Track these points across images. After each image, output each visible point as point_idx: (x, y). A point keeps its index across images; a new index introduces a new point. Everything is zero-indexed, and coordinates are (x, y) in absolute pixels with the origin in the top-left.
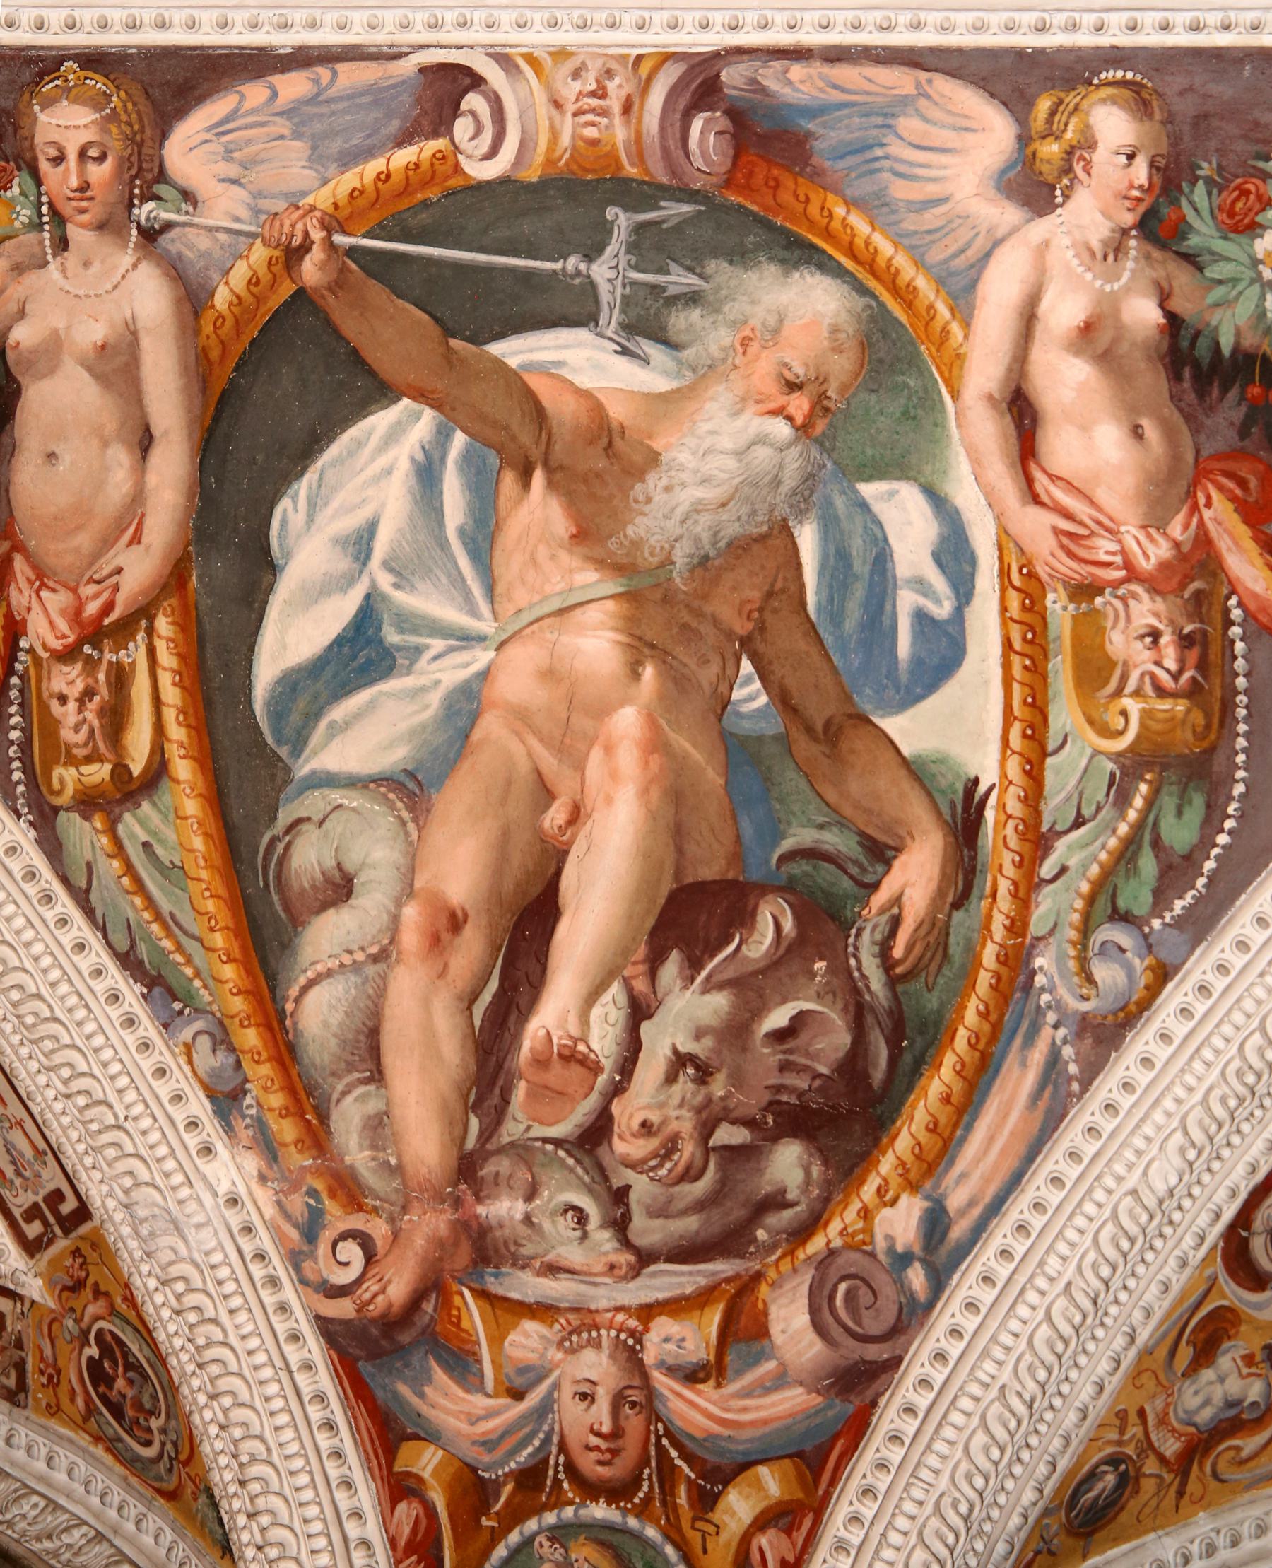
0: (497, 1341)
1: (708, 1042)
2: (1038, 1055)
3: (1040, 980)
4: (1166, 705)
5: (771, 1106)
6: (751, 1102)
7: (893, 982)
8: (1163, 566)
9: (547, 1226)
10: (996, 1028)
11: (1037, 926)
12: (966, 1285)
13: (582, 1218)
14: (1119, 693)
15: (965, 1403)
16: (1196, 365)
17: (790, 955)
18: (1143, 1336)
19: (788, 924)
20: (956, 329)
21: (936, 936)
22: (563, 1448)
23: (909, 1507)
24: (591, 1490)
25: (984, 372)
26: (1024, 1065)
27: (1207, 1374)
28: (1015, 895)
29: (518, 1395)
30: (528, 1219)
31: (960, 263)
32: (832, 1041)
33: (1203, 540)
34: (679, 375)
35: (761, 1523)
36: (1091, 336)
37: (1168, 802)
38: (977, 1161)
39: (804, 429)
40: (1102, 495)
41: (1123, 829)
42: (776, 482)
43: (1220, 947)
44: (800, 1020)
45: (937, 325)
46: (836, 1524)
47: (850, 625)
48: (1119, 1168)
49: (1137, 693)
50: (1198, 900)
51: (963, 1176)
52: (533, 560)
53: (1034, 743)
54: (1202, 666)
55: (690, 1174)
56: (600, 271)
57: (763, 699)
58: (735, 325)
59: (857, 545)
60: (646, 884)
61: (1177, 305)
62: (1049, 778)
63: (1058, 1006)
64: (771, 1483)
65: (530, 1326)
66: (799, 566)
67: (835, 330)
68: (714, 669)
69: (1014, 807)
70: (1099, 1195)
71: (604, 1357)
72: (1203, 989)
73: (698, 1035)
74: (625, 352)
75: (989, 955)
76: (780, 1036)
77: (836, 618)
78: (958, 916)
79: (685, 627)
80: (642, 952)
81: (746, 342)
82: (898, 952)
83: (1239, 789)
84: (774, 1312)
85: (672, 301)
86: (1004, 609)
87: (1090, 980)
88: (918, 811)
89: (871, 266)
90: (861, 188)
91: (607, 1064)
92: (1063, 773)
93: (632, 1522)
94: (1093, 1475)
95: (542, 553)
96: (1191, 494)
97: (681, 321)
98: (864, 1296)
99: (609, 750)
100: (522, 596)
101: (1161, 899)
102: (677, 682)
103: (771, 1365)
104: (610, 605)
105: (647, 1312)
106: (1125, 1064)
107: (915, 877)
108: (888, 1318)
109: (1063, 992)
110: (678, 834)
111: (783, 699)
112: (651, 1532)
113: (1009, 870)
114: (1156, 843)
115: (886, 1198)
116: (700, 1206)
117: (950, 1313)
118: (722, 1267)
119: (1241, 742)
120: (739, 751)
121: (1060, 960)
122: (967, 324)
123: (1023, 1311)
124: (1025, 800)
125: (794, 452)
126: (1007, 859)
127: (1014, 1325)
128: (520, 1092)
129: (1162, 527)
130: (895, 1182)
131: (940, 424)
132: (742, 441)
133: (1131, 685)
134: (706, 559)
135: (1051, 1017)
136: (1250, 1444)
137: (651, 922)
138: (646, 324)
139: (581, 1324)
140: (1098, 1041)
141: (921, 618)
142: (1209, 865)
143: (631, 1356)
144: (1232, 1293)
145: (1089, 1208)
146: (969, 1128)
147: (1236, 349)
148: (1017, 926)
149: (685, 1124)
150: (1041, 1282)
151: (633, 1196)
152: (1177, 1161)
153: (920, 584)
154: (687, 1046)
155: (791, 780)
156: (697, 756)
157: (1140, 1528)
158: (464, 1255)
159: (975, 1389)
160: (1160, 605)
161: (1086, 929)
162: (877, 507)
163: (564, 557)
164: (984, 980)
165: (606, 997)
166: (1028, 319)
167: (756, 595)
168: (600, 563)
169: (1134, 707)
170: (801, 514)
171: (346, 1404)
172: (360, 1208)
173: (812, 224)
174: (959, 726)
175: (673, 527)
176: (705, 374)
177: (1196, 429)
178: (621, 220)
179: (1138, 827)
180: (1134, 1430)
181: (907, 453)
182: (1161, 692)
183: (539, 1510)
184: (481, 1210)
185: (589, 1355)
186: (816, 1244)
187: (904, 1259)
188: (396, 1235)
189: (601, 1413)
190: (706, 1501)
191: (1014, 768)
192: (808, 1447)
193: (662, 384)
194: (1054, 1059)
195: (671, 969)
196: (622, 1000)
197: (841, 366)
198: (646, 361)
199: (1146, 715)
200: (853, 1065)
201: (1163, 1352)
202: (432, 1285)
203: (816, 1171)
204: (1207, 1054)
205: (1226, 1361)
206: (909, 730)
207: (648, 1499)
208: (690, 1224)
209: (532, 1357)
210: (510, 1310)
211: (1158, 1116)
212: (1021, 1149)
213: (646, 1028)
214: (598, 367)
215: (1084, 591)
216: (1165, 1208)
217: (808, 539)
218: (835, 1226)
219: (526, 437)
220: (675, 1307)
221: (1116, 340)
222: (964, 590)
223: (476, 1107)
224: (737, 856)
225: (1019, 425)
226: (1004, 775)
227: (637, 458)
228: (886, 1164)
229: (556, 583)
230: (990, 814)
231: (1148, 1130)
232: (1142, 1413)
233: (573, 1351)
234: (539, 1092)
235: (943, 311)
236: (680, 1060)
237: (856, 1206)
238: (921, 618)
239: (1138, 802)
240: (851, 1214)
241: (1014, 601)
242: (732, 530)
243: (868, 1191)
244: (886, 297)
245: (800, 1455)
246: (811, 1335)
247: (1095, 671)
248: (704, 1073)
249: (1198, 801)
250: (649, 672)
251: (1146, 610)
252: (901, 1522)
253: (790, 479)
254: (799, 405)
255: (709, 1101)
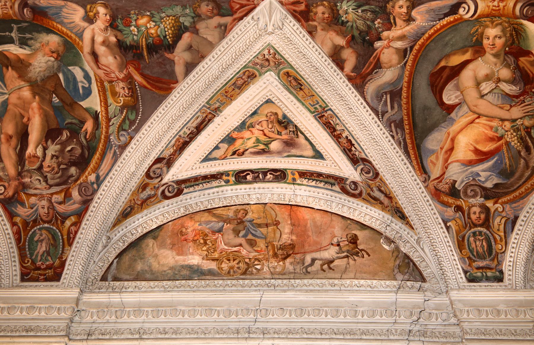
0: (28, 200)
1: (57, 153)
2: (112, 151)
3: (111, 140)
4: (127, 98)
5: (69, 162)
6: (66, 161)
7: (87, 142)
8: (123, 78)
9: (34, 182)
10: (105, 148)
11: (110, 132)
12: (103, 187)
13: (40, 181)
14: (119, 97)
15: (103, 205)
16: (124, 47)
17: (69, 140)
18: (133, 189)
19: (68, 134)
20: (80, 42)
21: (93, 135)
22: (40, 216)
23: (94, 222)
24: (45, 222)
25: (87, 49)
26: (110, 153)
27: (145, 192)
28: (106, 128)
29: (32, 208)
30: (31, 181)
31: (79, 32)
32: (79, 151)
33: (129, 73)
34: (32, 51)
35: (71, 225)
36: (105, 43)
37: (129, 113)
38: (104, 168)
39: (56, 59)
40: (111, 67)
41: (122, 117)
42: (53, 67)
43: (140, 134)
44: (72, 149)
45: (77, 42)
46: (83, 225)
47: (71, 89)
48: (126, 168)
49: (122, 97)
50: (136, 127)
51: (102, 170)
52: (12, 81)
53: (106, 105)
54: (132, 92)
55: (57, 173)
56: (13, 35)
57: (58, 100)
58: (41, 43)
59: (70, 76)
60: (43, 129)
61: (119, 38)
62: (109, 110)
63: (115, 144)
64: (73, 219)
65: (33, 197)
66: (60, 80)
67: (58, 43)
68: (48, 96)
69: (104, 114)
70: (123, 172)
71: (46, 202)
72: (138, 141)
73: (56, 152)
74: (21, 47)
75: (103, 137)
76: (69, 151)
77: (69, 88)
78: (97, 131)
79: (42, 90)
80: (44, 140)
81: (43, 45)
82: (87, 137)
83: (141, 110)
84: (73, 193)
85: (28, 39)
86: (97, 85)
87: (120, 140)
88: (88, 116)
89: (63, 32)
90: (58, 20)
91: (41, 157)
92: (111, 109)
93: (51, 227)
94: (126, 209)
95: (13, 80)
96: (126, 67)
97: (30, 42)
98: (87, 189)
99: (32, 109)
100: (11, 87)
101: (130, 127)
102: (42, 99)
103: (72, 201)
104: (28, 87)
105: (52, 194)
106: (126, 152)
107: (89, 126)
108: (91, 193)
109: (115, 142)
110: (47, 121)
111: (61, 100)
112: (54, 228)
113: (104, 124)
114: (128, 119)
115: (89, 174)
116: (59, 178)
117: (100, 191)
118: (64, 187)
119: (140, 103)
120: (55, 108)
121: (115, 137)
122: (82, 41)
123: (111, 191)
124: (106, 114)
125: (56, 62)
126: (104, 122)
127: (110, 193)
128: (27, 162)
129: (122, 72)
130: (91, 172)
131: (80, 57)
132: (46, 61)
133: (121, 95)
134: (43, 79)
135: (114, 146)
136: (152, 200)
137: (45, 135)
138: (23, 43)
139: (41, 197)
140: (122, 149)
141: (83, 87)
142: (137, 121)
143: (50, 201)
144: (147, 181)
145: (121, 174)
146: (102, 163)
147: (130, 44)
148: (107, 132)
149: (55, 165)
150: (114, 186)
151: (48, 177)
152: (135, 167)
153: (82, 82)
154: (54, 153)
155: (65, 112)
156: (48, 109)
157: (135, 214)
158: (21, 188)
159: (104, 203)
160: (124, 83)
161: (118, 132)
162: (72, 70)
163: (18, 80)
164: (102, 141)
165: (39, 147)
166: (93, 41)
167: (53, 85)
168: (24, 81)
169: (122, 99)
170: (59, 72)
171: (4, 211)
172: (2, 181)
173: (51, 26)
174: (94, 102)
175: (36, 75)
176: (36, 51)
177: (125, 57)
178: (15, 27)
179: (125, 117)
180: (133, 202)
181: (77, 61)
182: (126, 96)
183: (37, 226)
184: (23, 180)
185: (43, 201)
186: (79, 182)
187: (93, 183)
188: (9, 185)
189: (46, 210)
190: (63, 223)
191: (103, 109)
192: (79, 213)
193: (29, 53)
194: (115, 152)
195: (49, 142)
196: (42, 147)
197: (61, 49)
198: (25, 49)
199: (124, 100)
200: (82, 154)
201: (137, 190)
202: (16, 192)
203: (78, 171)
204: (139, 150)
205: (147, 190)
206: (84, 104)
207: (54, 223)
208: (58, 180)
209: (34, 202)
210: (29, 195)
211: (132, 160)
212: (111, 165)
213: (46, 151)
214: (16, 50)
215: (110, 82)
216: (133, 174)
217: (61, 76)
218: (81, 179)
219: (6, 61)
220: (56, 193)
221: (109, 43)
222: (90, 82)
223: (20, 165)
224: (58, 124)
225: (95, 57)
226: (101, 110)
227: (27, 64)
228: (89, 169)
229: (17, 84)
230: (100, 116)
231: (130, 162)
232: (134, 199)
233: (40, 201)
234: (29, 162)
235: (78, 40)
236: (53, 156)
237: (85, 176)
238: (83, 87)
239: (125, 113)
240: (84, 177)
241: (99, 84)
242: (47, 75)
243: (87, 173)
244: (67, 38)
245: (77, 214)
246: (79, 196)
247: (114, 94)
248: (57, 158)
249: (134, 112)
250: (37, 97)
251: (121, 84)
252: (93, 224)
253: (56, 67)
254: (55, 55)
255: (59, 162)
